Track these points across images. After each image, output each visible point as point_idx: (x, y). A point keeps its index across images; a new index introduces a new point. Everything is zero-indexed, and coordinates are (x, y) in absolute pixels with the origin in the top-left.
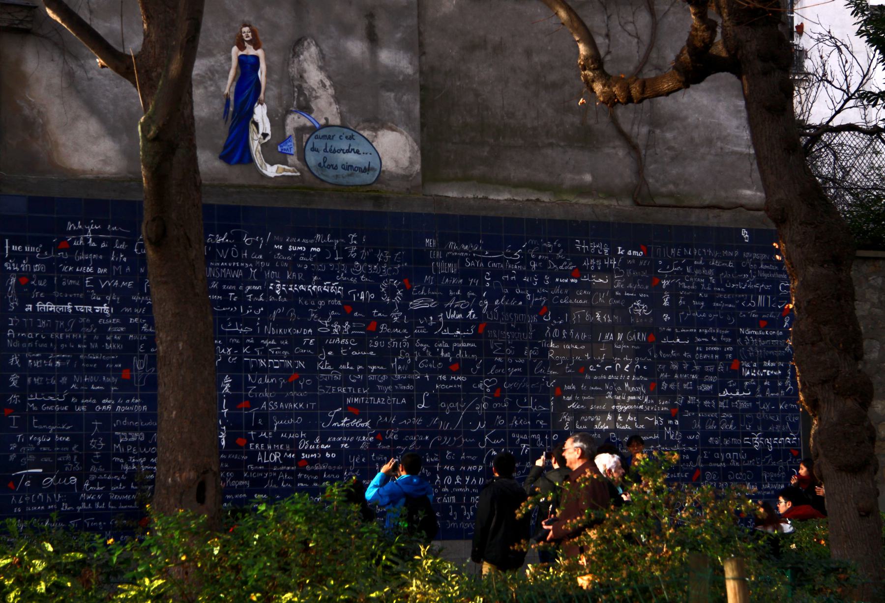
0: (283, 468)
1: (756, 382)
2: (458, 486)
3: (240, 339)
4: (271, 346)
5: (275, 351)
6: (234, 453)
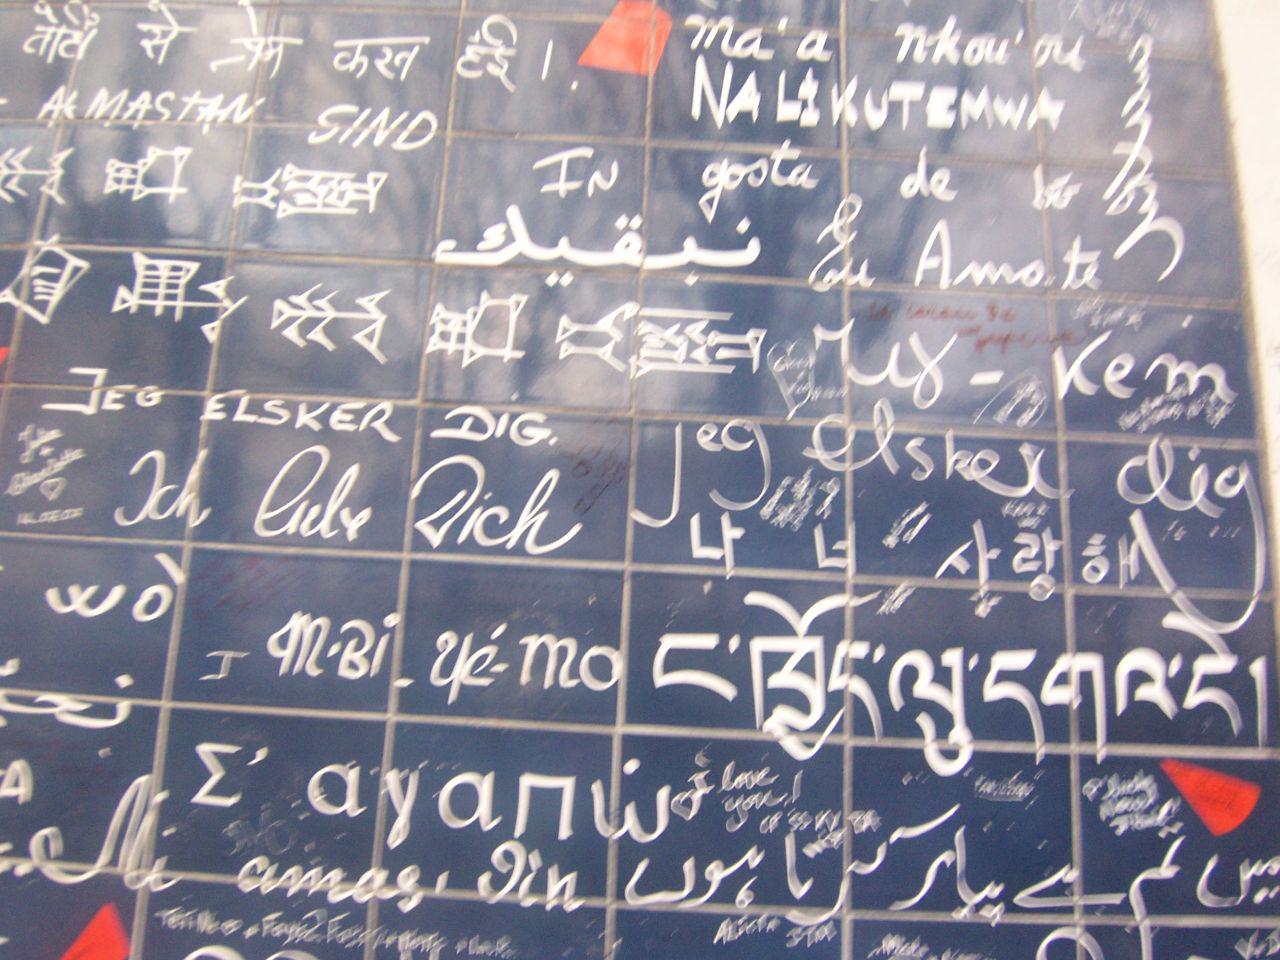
1: (828, 175)
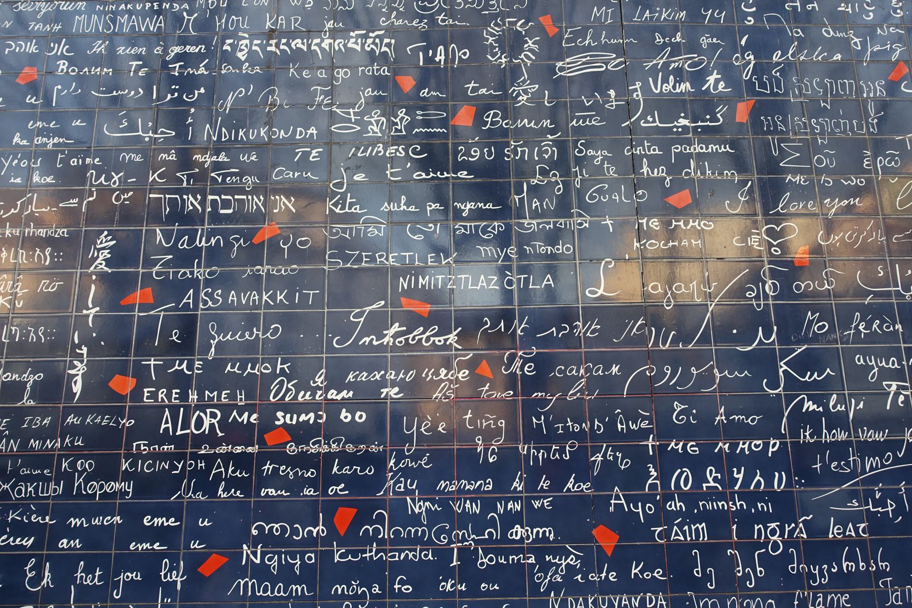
0: (223, 449)
2: (713, 495)
3: (144, 152)
4: (217, 166)
5: (225, 176)
6: (102, 411)
